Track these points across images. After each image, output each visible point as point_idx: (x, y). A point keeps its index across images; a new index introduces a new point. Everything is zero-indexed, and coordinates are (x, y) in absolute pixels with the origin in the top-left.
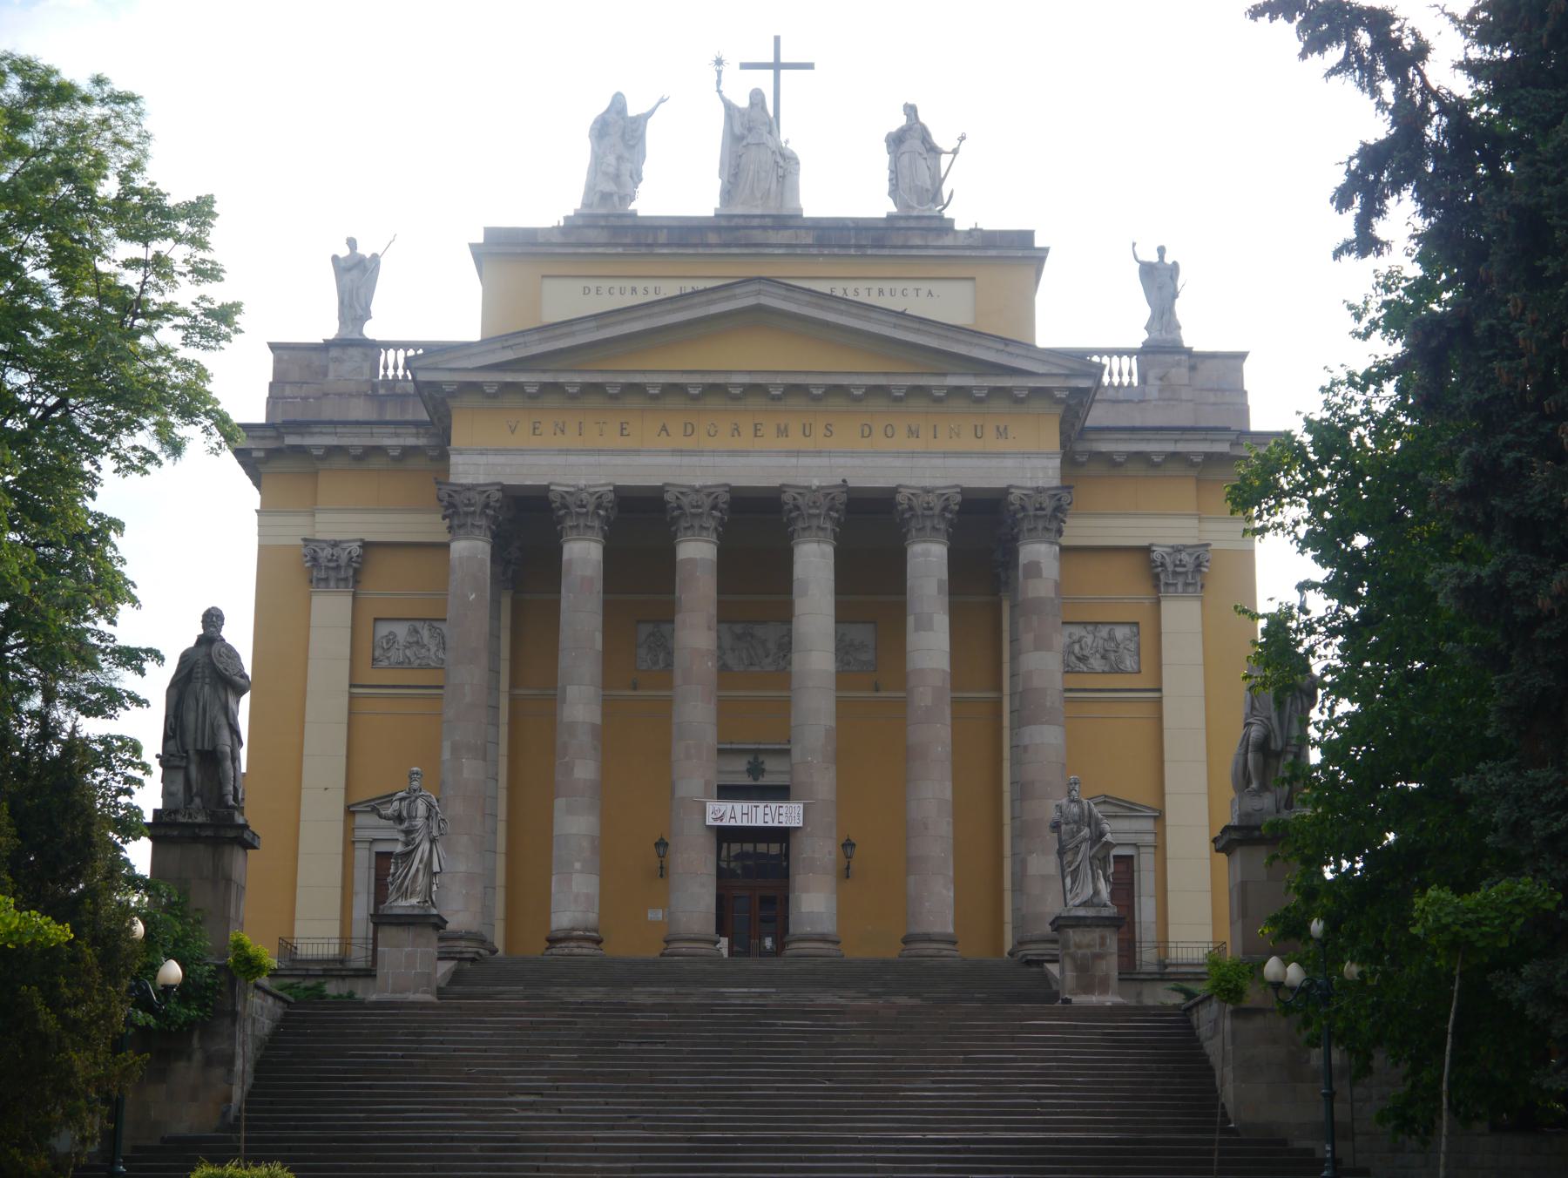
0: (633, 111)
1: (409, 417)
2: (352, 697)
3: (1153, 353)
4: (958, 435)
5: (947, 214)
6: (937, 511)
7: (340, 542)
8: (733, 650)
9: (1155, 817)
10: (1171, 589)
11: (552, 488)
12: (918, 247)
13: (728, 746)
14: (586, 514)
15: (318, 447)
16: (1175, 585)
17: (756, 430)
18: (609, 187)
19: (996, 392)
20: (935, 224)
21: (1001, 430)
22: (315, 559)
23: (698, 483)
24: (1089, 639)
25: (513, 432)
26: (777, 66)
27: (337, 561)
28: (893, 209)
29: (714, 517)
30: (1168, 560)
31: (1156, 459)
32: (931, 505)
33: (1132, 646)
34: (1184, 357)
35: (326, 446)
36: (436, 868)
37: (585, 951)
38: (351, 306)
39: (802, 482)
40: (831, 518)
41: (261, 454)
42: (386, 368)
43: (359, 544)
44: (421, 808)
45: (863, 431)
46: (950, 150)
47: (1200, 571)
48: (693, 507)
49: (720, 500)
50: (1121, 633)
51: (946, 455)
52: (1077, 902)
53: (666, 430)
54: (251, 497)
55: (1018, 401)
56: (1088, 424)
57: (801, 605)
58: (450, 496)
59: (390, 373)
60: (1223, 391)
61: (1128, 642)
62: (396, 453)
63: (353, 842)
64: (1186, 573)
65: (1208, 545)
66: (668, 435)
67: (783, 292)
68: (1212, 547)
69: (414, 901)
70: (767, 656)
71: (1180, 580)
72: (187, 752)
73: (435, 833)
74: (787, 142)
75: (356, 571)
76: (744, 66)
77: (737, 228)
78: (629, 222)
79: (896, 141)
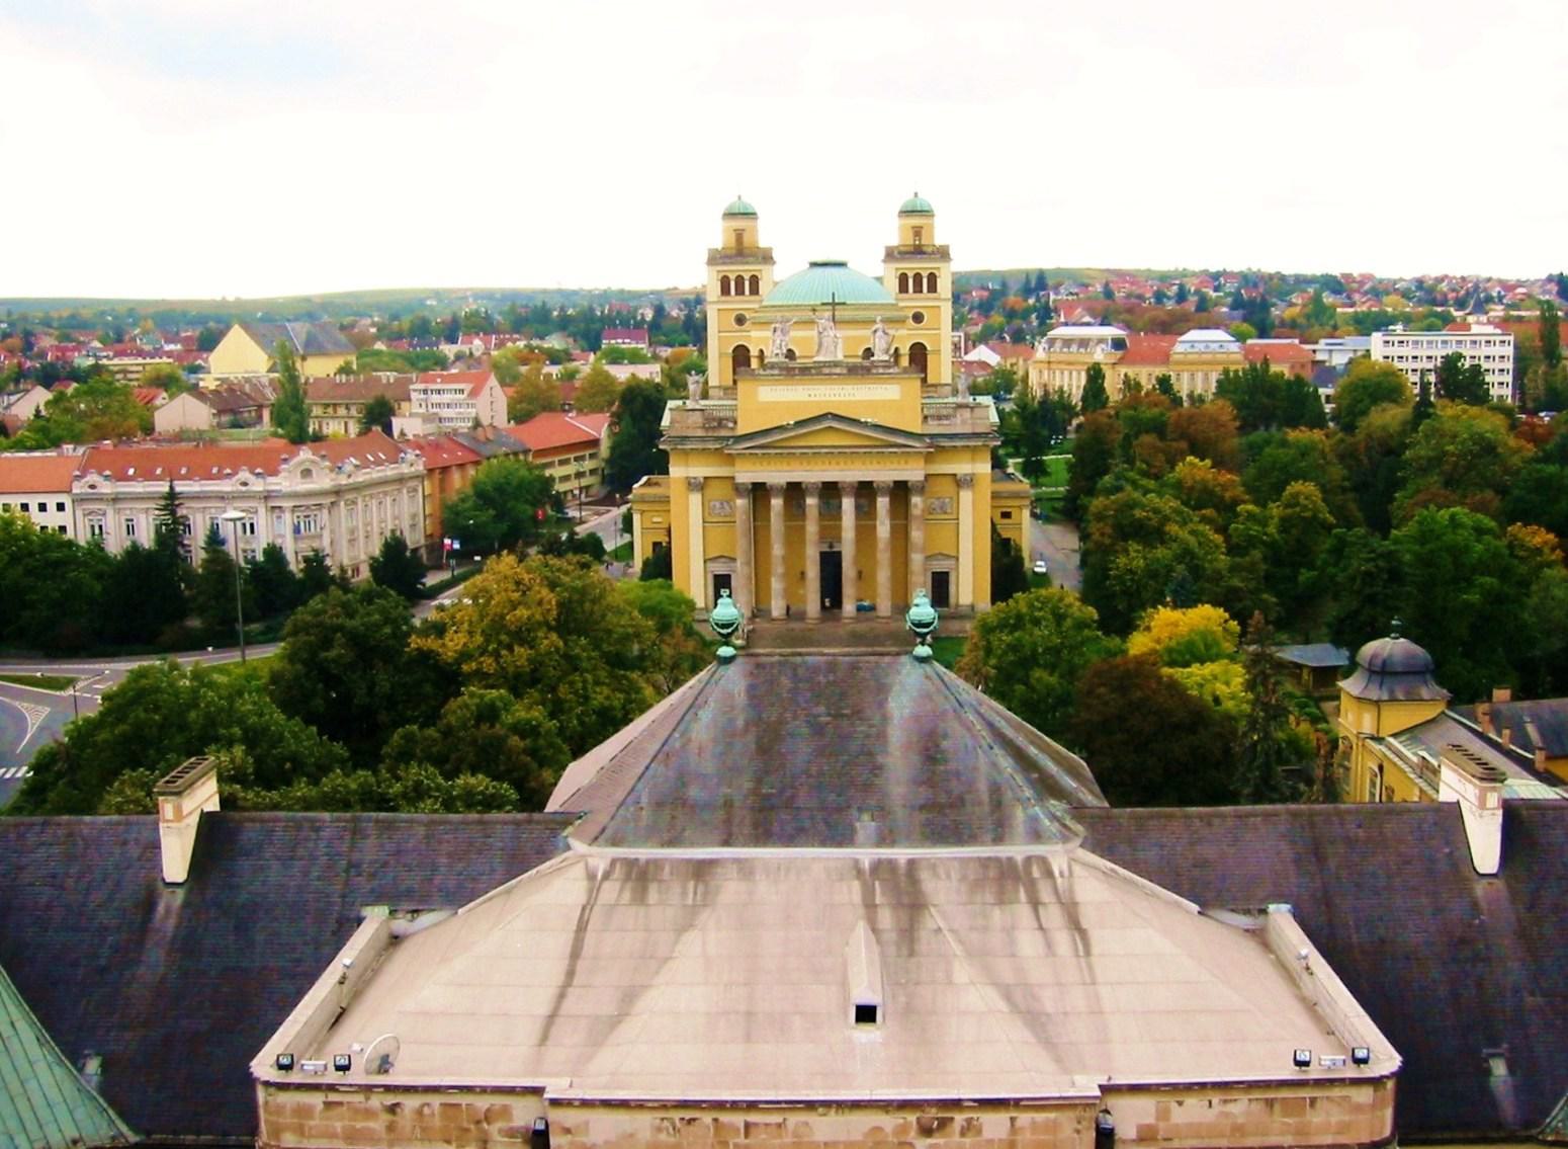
2: (704, 527)
50: (947, 500)
57: (844, 518)
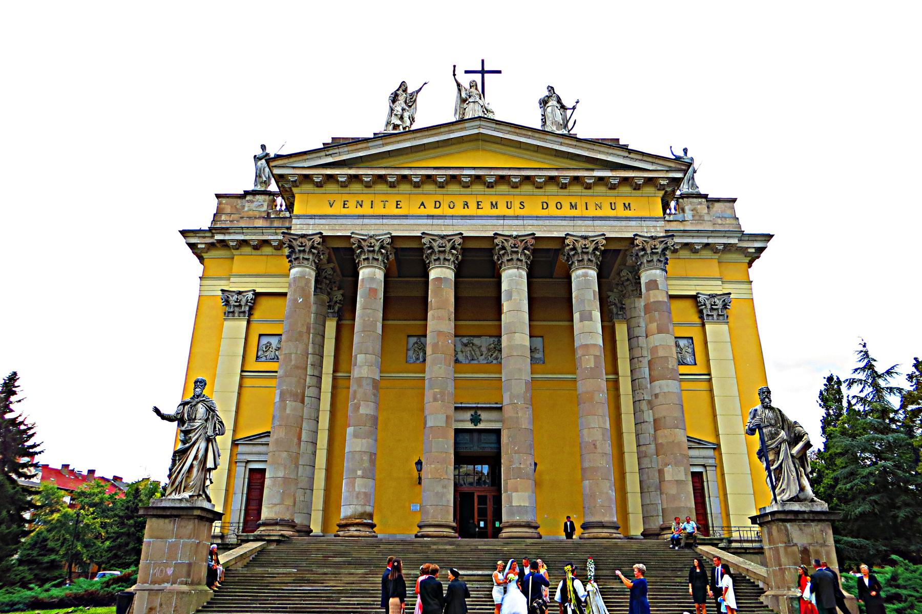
0: (410, 91)
3: (687, 197)
6: (590, 250)
7: (243, 292)
8: (462, 352)
9: (714, 449)
11: (353, 236)
14: (373, 251)
15: (233, 240)
16: (713, 315)
17: (478, 205)
19: (625, 180)
21: (627, 205)
22: (227, 302)
25: (331, 207)
26: (483, 72)
27: (240, 302)
31: (697, 247)
32: (587, 246)
33: (690, 350)
36: (210, 464)
37: (363, 534)
38: (260, 177)
41: (203, 246)
42: (276, 206)
44: (201, 410)
46: (571, 107)
47: (727, 308)
48: (440, 247)
52: (786, 497)
58: (290, 241)
59: (278, 208)
60: (726, 218)
61: (687, 348)
62: (276, 244)
63: (236, 462)
64: (717, 309)
65: (730, 294)
66: (425, 208)
67: (494, 126)
68: (732, 296)
70: (482, 355)
71: (715, 313)
74: (488, 104)
75: (251, 308)
76: (467, 72)
79: (544, 102)
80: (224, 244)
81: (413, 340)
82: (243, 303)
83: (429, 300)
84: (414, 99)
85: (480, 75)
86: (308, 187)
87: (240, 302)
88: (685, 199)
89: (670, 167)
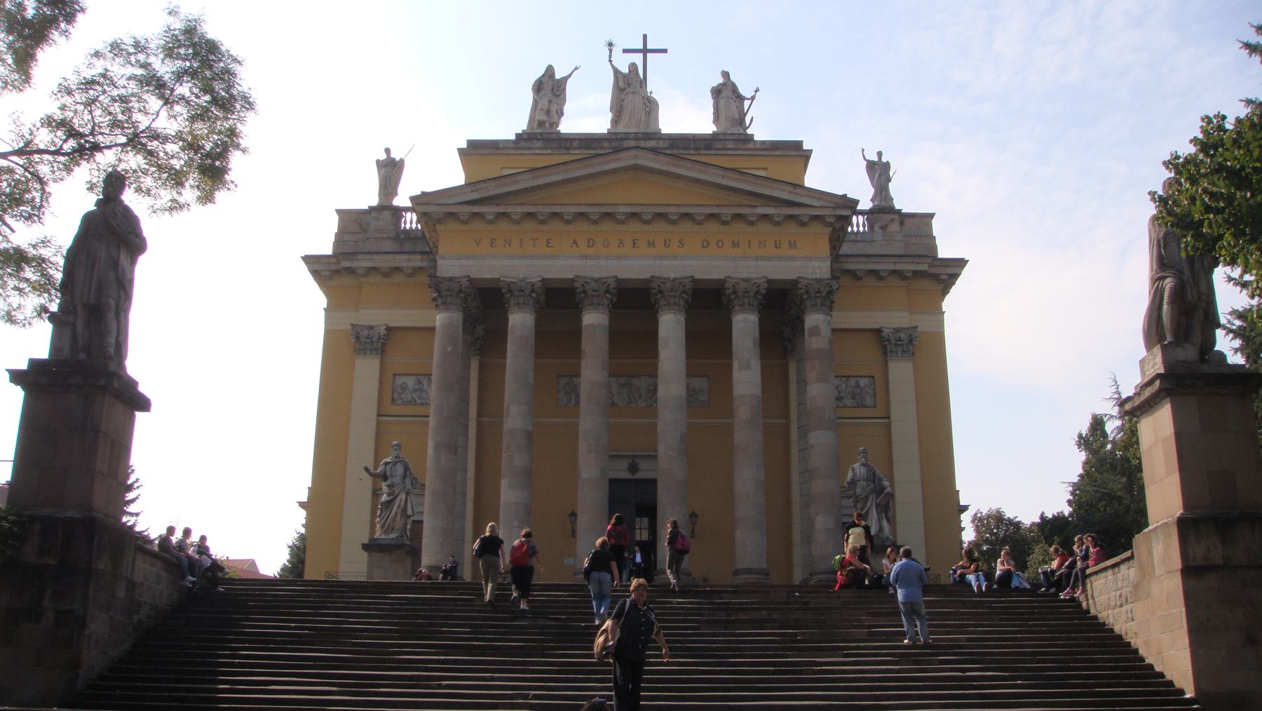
0: (558, 76)
1: (419, 249)
2: (378, 423)
4: (765, 246)
5: (749, 131)
6: (752, 294)
10: (894, 355)
12: (732, 149)
13: (616, 453)
18: (543, 117)
19: (790, 217)
20: (742, 137)
21: (792, 243)
22: (357, 337)
23: (596, 276)
24: (844, 387)
25: (478, 245)
26: (645, 51)
28: (716, 130)
29: (607, 298)
30: (892, 337)
32: (748, 290)
34: (896, 216)
35: (366, 268)
36: (409, 512)
39: (665, 275)
40: (683, 298)
42: (405, 223)
43: (385, 327)
44: (400, 469)
45: (703, 244)
47: (912, 344)
49: (611, 286)
50: (863, 382)
51: (757, 258)
53: (576, 244)
54: (320, 300)
55: (803, 224)
56: (840, 253)
58: (436, 285)
60: (921, 236)
61: (867, 389)
64: (903, 345)
65: (916, 327)
69: (393, 536)
70: (640, 397)
71: (900, 348)
72: (75, 307)
73: (409, 486)
74: (651, 93)
75: (383, 344)
76: (625, 51)
77: (621, 139)
78: (553, 136)
79: (717, 92)
80: (350, 271)
81: (563, 381)
82: (375, 339)
83: (583, 347)
84: (562, 88)
85: (641, 55)
86: (451, 225)
87: (371, 338)
88: (875, 215)
89: (837, 204)
